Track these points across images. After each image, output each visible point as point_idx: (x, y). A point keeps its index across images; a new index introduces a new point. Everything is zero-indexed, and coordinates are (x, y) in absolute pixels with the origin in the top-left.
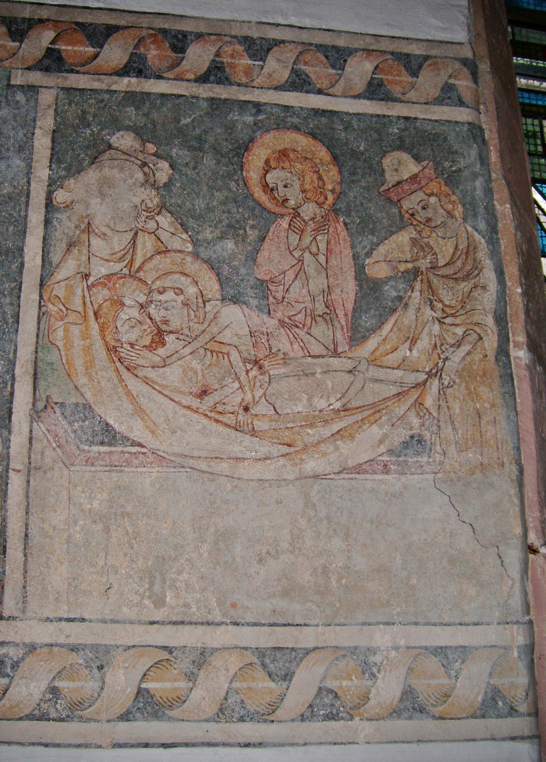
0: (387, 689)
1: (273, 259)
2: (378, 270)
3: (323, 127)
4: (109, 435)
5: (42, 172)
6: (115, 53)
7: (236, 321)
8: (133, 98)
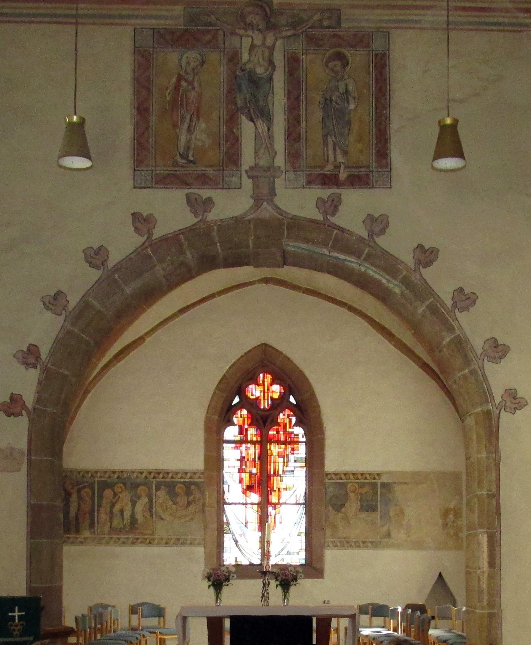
0: (189, 542)
1: (178, 499)
2: (190, 500)
3: (183, 483)
4: (162, 519)
5: (154, 491)
6: (161, 476)
7: (174, 507)
8: (164, 482)
